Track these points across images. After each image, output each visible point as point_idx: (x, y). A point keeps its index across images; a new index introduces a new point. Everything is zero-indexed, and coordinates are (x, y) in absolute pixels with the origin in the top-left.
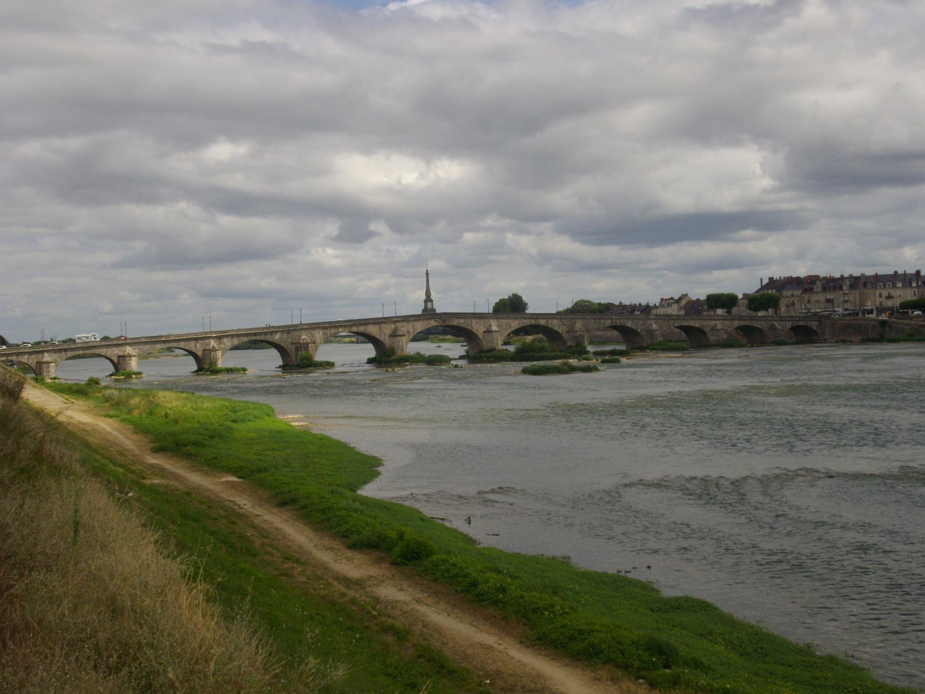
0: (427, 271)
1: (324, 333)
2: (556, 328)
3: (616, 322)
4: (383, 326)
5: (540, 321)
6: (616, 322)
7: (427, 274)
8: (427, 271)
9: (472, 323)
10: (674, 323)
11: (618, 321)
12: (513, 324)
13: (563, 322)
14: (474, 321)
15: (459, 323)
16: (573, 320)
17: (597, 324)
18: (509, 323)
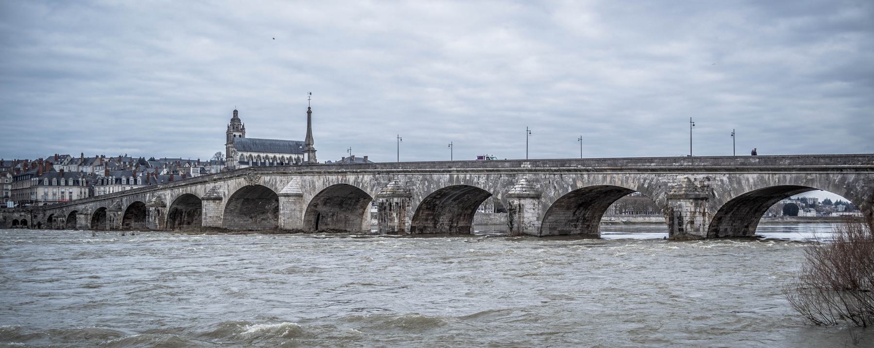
0: (309, 108)
1: (172, 195)
2: (368, 191)
3: (458, 177)
4: (207, 185)
5: (348, 177)
6: (458, 177)
7: (309, 112)
8: (309, 108)
9: (276, 182)
10: (574, 180)
11: (462, 176)
12: (317, 183)
13: (377, 180)
14: (278, 178)
15: (265, 182)
16: (391, 175)
17: (427, 184)
18: (313, 182)
